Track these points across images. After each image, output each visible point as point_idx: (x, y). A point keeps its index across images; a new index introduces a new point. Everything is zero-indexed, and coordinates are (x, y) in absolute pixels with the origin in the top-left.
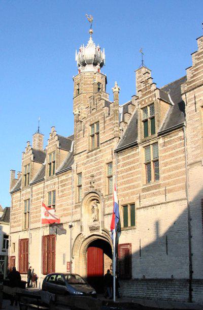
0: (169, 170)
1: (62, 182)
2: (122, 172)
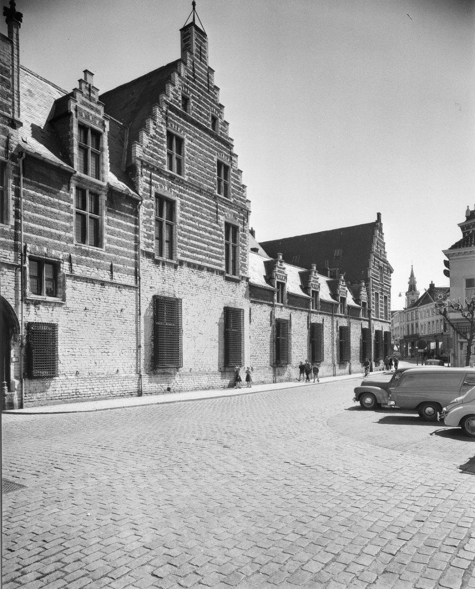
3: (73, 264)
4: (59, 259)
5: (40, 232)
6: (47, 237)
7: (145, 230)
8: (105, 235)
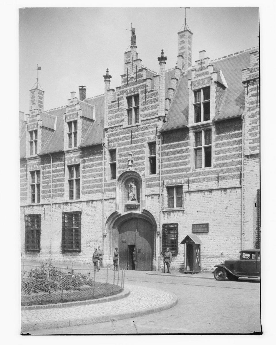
3: (190, 184)
4: (182, 184)
5: (171, 171)
6: (175, 173)
7: (250, 137)
8: (213, 155)
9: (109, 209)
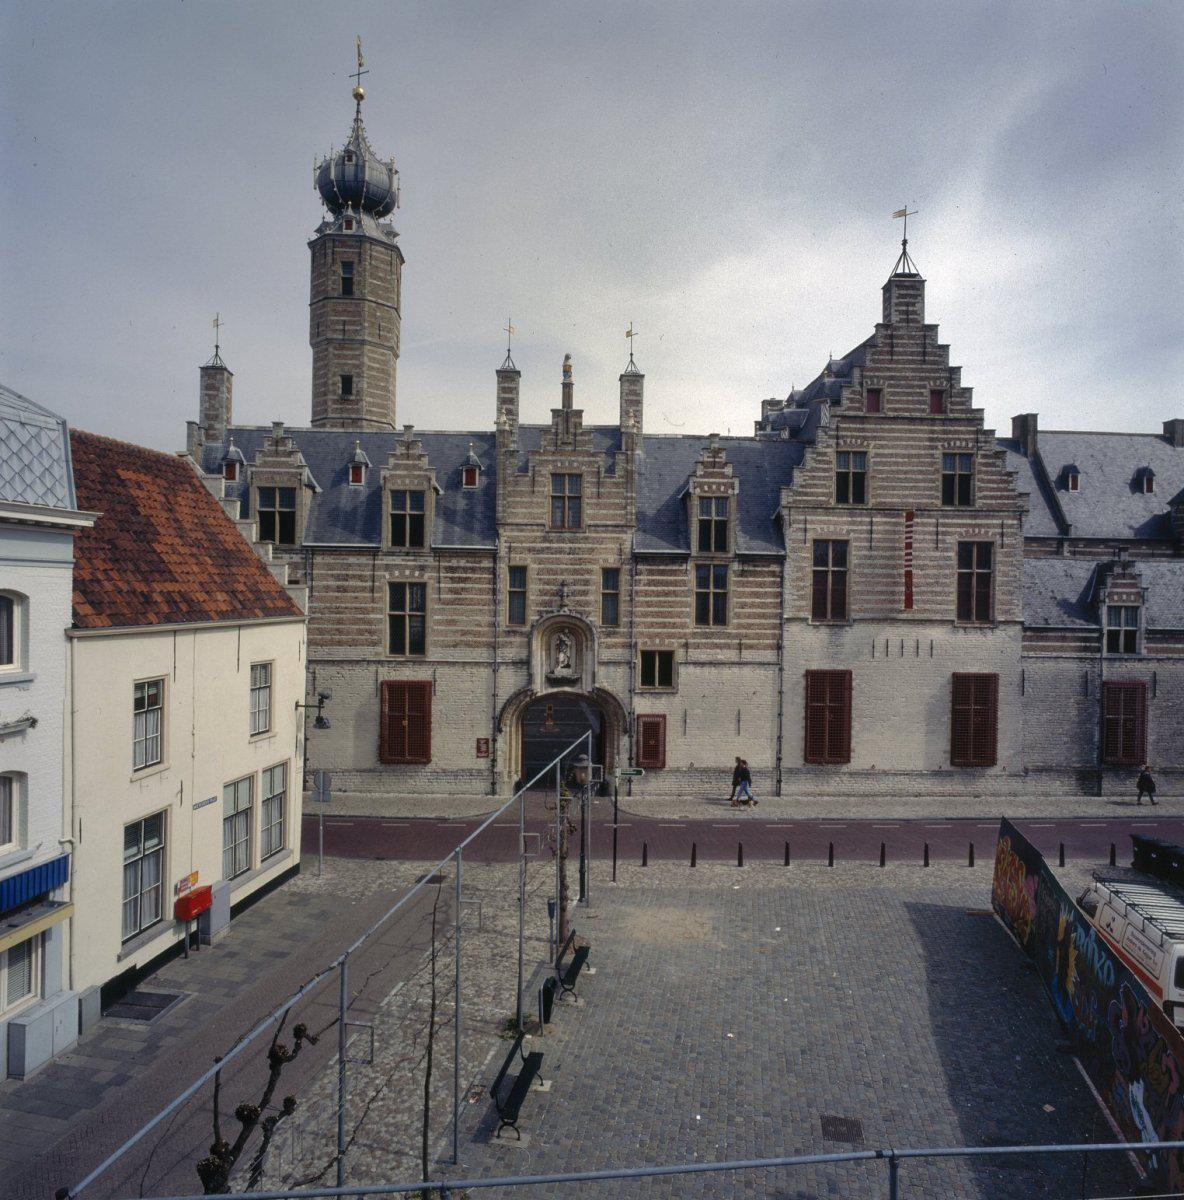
0: (749, 616)
1: (452, 569)
2: (647, 594)
9: (509, 681)
